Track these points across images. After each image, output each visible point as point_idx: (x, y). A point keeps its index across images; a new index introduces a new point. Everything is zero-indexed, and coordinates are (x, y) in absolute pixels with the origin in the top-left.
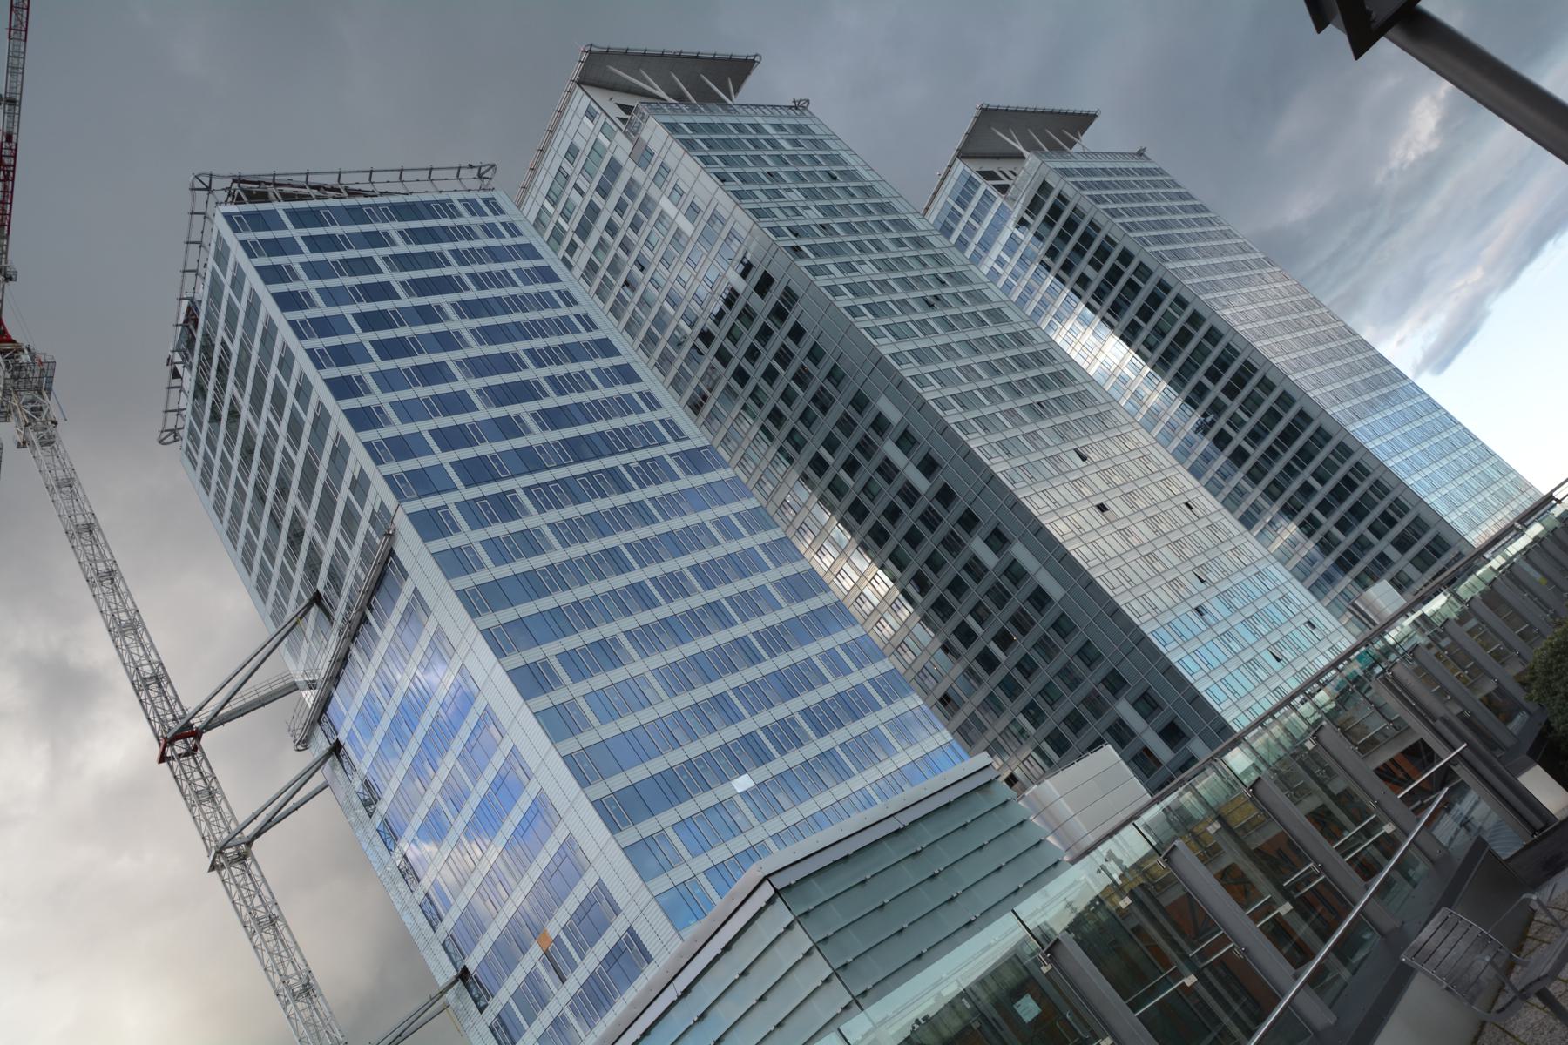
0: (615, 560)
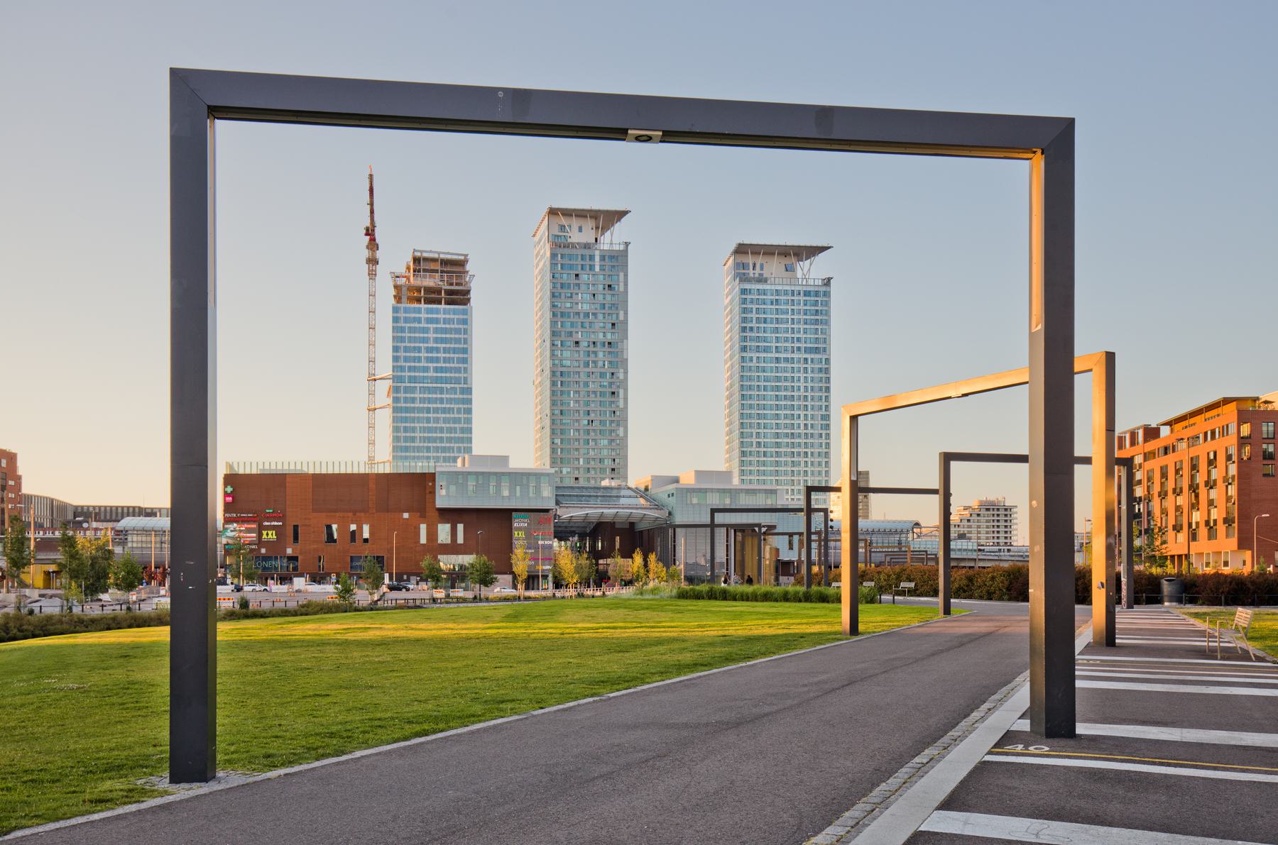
0: (428, 410)
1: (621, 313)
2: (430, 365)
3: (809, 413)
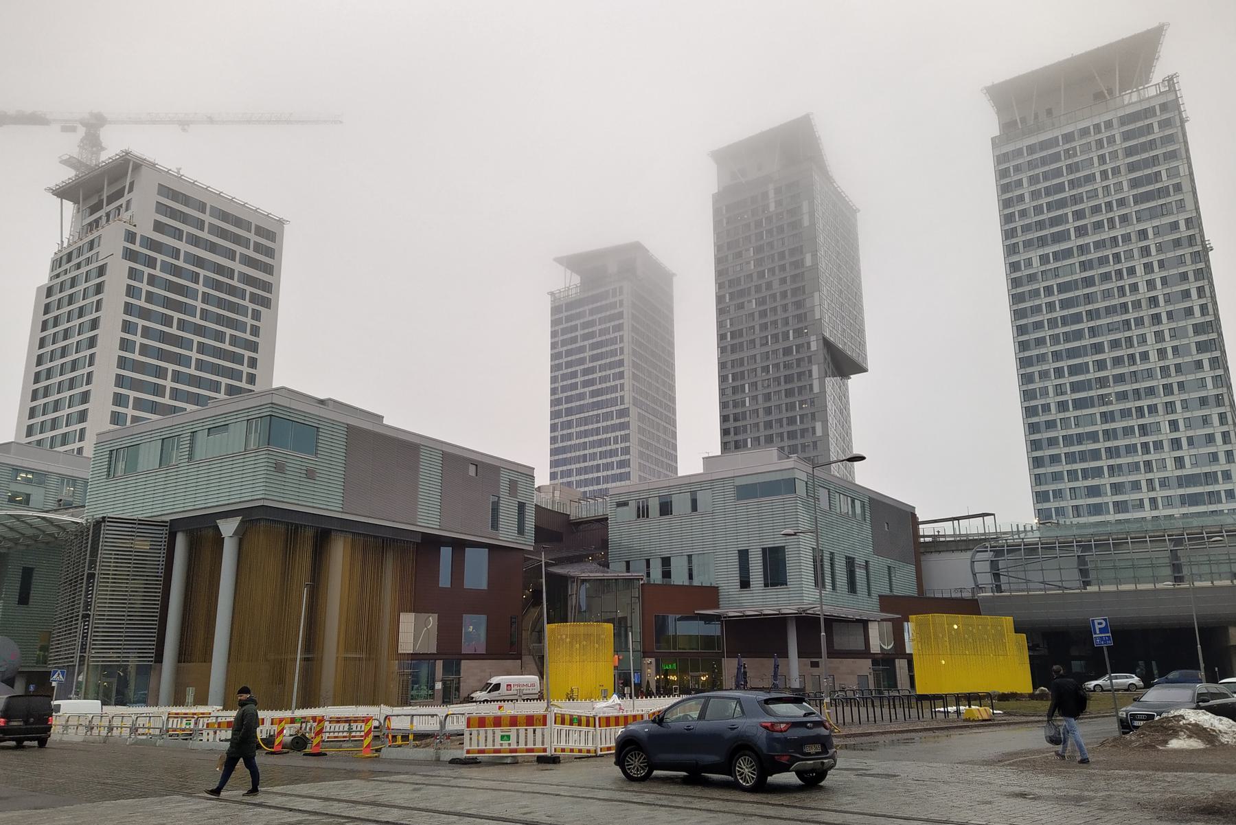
3: (1166, 326)
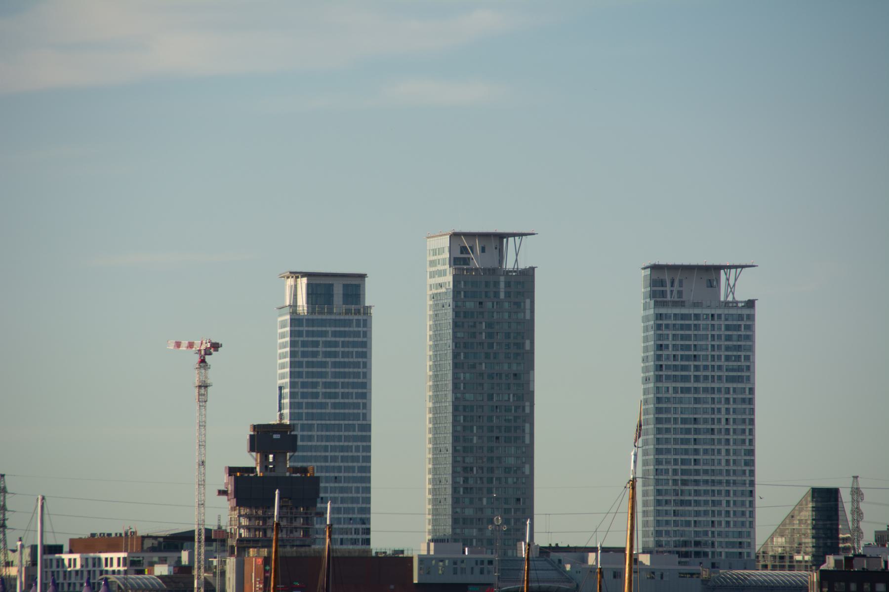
0: (325, 449)
1: (528, 342)
2: (328, 401)
